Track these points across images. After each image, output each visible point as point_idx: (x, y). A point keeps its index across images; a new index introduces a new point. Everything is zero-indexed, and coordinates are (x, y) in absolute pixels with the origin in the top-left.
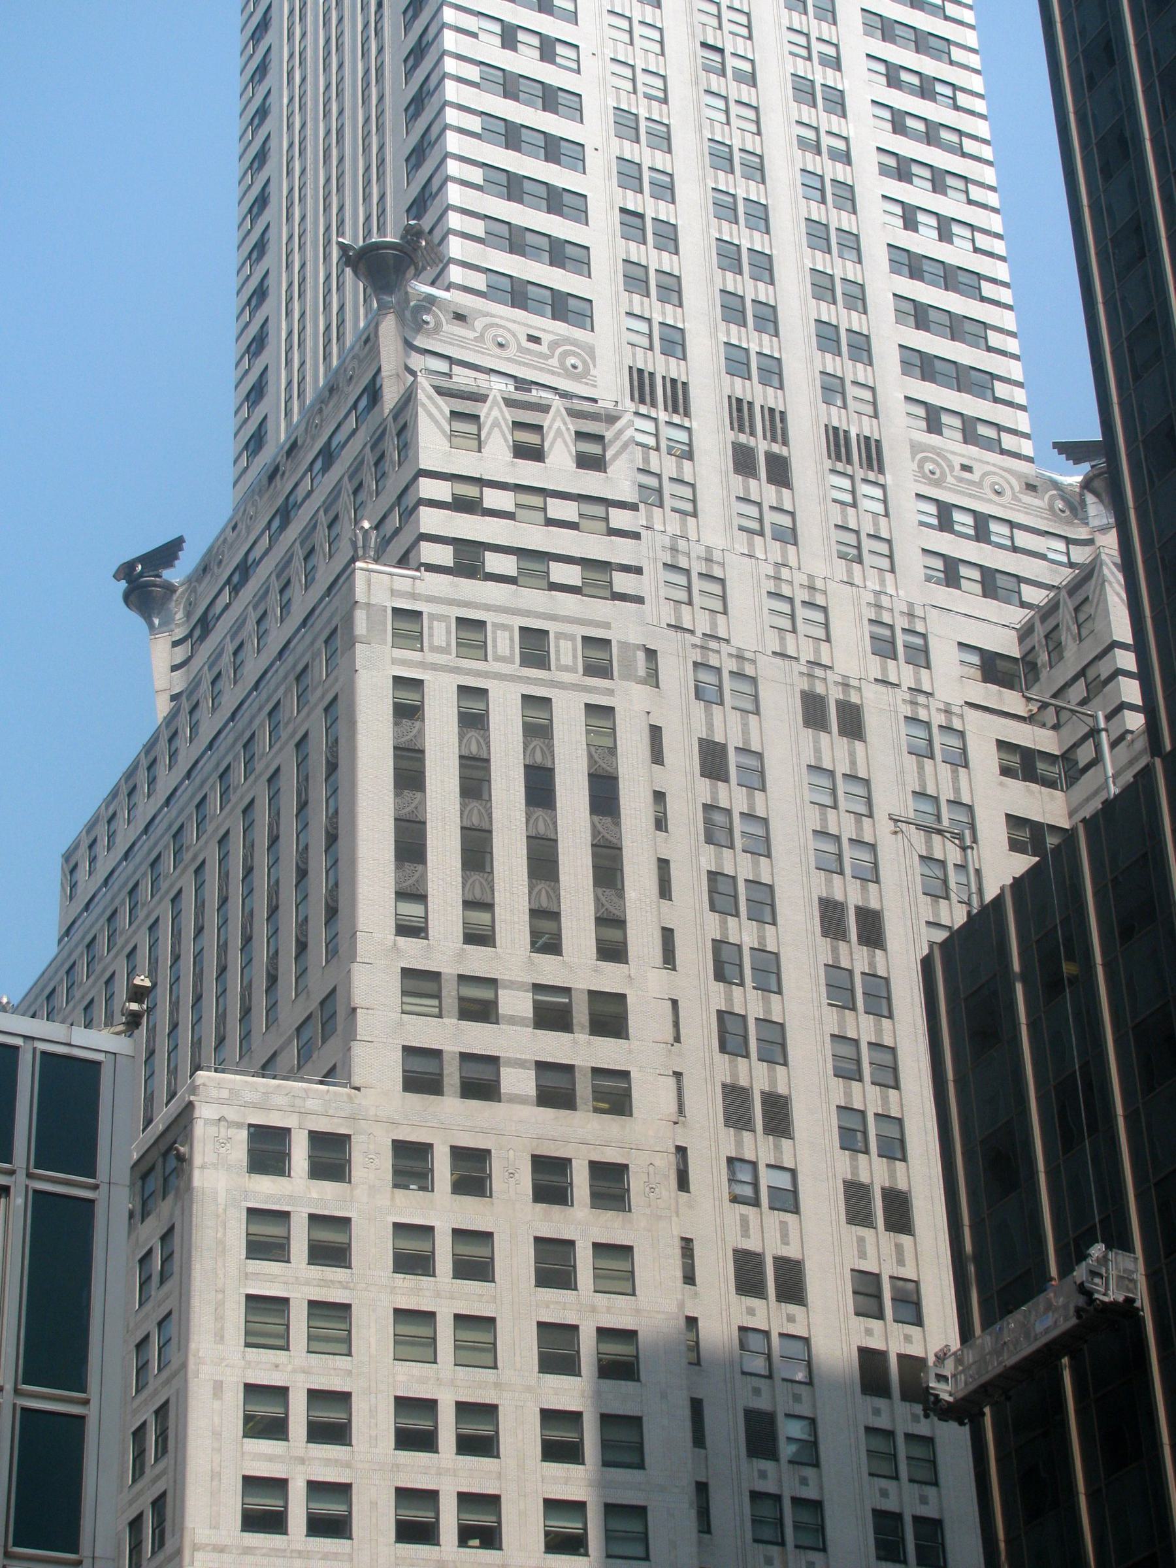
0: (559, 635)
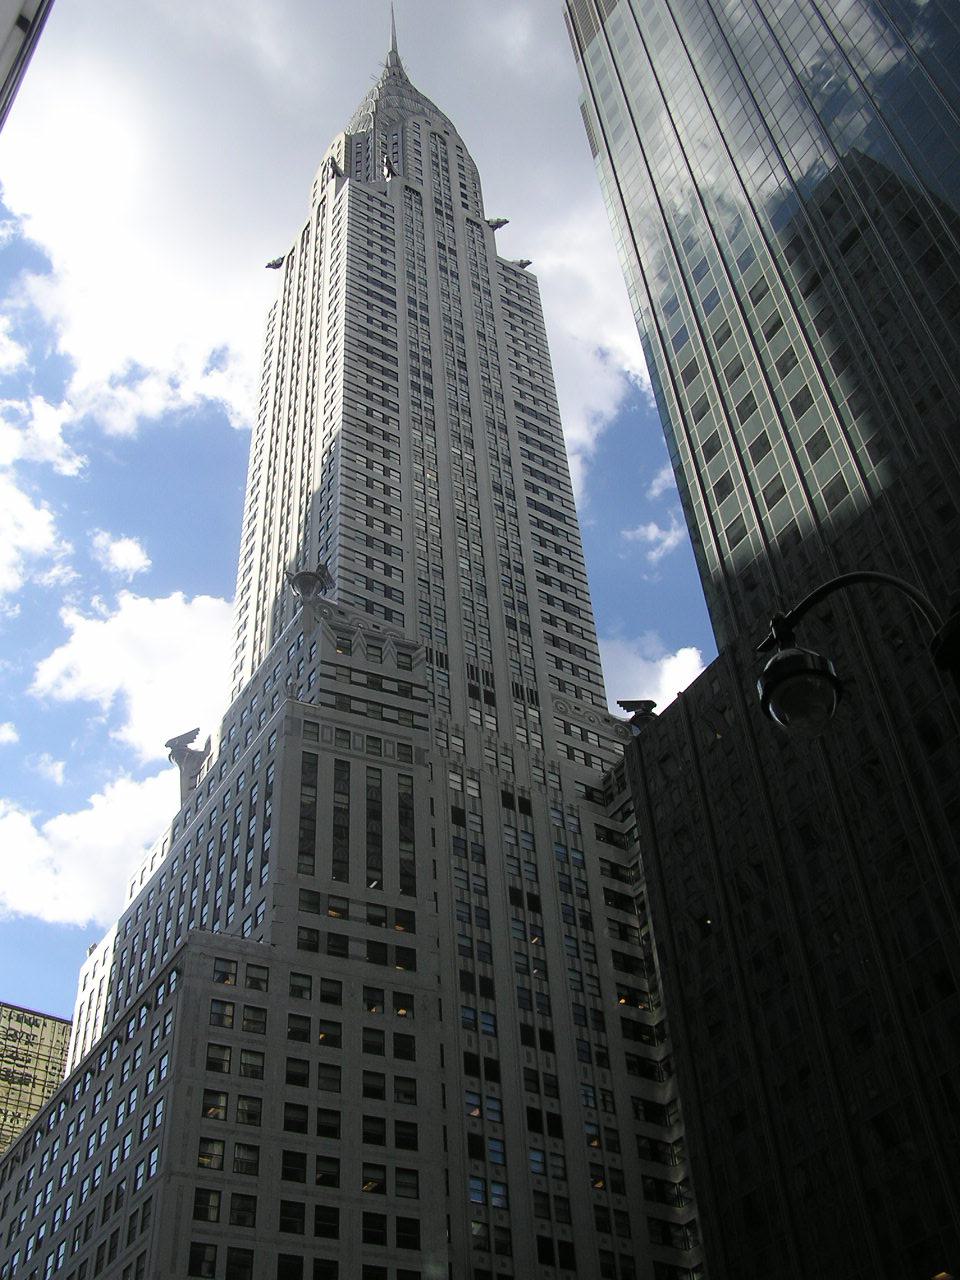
0: (387, 741)
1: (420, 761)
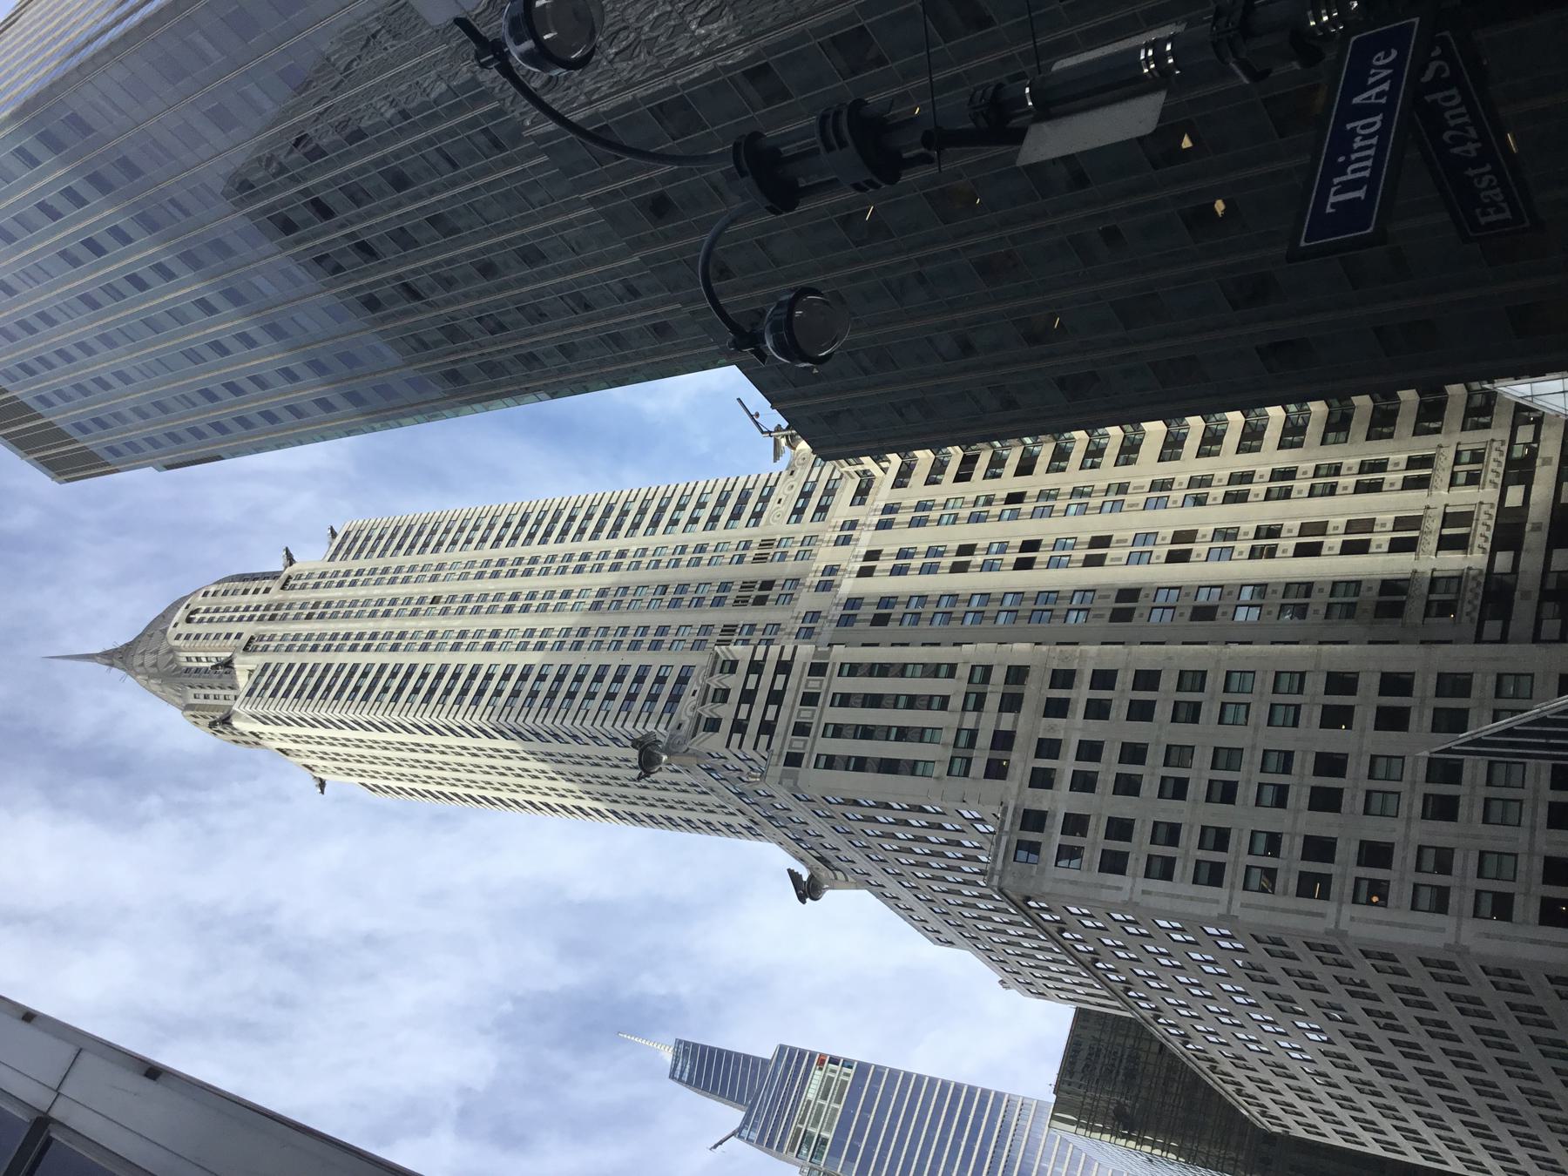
1: (827, 655)
